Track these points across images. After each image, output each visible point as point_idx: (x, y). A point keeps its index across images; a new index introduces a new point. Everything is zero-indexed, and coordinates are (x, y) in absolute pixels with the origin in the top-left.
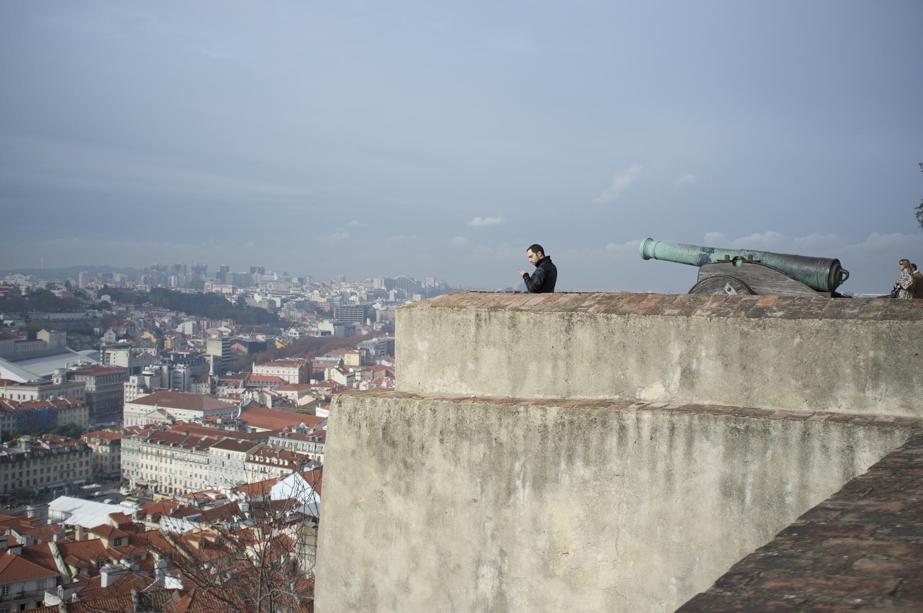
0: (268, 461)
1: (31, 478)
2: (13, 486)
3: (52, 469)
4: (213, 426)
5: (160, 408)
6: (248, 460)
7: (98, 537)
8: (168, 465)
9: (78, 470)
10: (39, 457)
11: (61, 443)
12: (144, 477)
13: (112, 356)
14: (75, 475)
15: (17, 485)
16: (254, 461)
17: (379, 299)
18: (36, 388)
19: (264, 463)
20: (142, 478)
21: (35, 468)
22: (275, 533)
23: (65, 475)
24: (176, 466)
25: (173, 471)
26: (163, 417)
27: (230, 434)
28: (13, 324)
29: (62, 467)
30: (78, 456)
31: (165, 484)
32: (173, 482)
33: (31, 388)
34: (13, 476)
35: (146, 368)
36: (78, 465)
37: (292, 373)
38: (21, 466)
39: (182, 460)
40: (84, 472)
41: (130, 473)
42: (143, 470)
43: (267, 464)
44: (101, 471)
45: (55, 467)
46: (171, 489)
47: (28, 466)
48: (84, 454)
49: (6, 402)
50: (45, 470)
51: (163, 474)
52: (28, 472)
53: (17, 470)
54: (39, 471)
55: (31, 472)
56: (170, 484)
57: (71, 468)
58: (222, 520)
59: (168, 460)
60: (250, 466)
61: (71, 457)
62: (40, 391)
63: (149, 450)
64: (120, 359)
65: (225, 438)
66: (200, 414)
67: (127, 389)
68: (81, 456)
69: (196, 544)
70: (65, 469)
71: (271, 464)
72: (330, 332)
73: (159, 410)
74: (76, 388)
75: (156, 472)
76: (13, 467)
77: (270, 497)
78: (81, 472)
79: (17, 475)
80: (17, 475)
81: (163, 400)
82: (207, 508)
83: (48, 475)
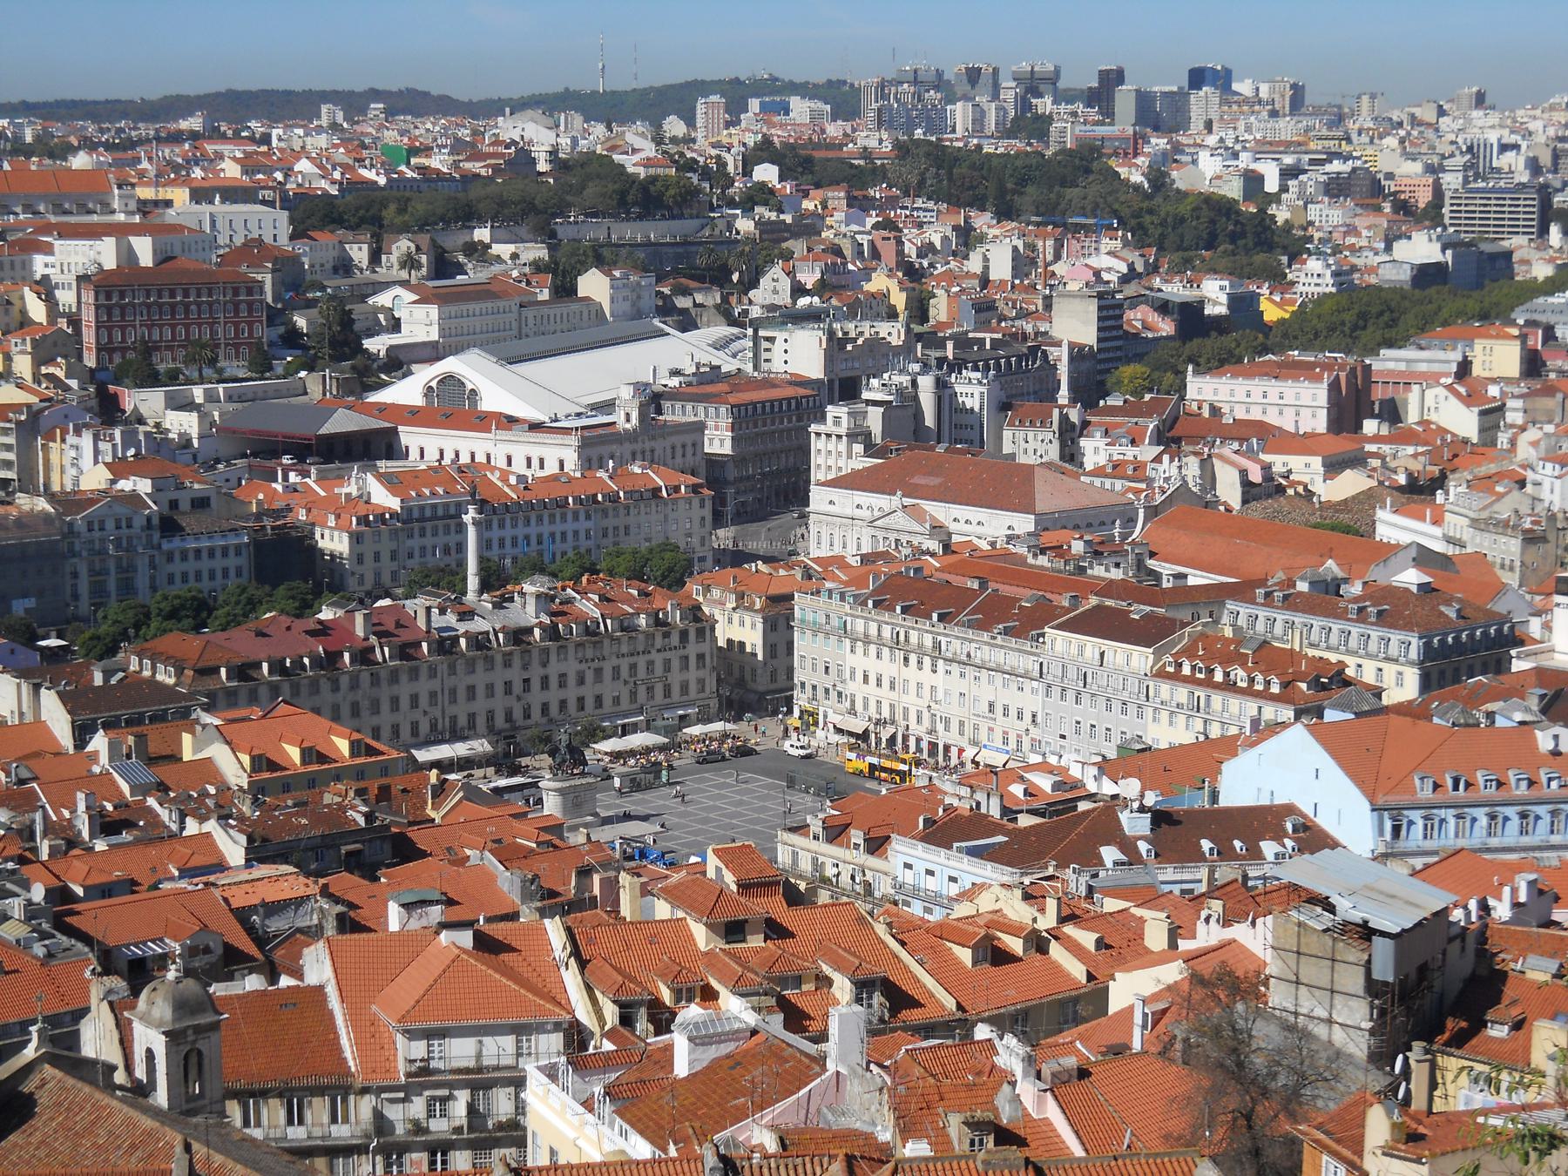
0: (1219, 677)
4: (1060, 564)
5: (907, 501)
6: (1161, 674)
7: (680, 914)
8: (926, 676)
9: (675, 678)
11: (629, 600)
12: (859, 707)
13: (779, 346)
14: (667, 692)
16: (1176, 677)
19: (1208, 683)
20: (852, 711)
21: (562, 668)
22: (1208, 935)
23: (642, 691)
24: (946, 681)
25: (940, 695)
26: (918, 528)
27: (1109, 588)
28: (515, 256)
31: (917, 730)
32: (940, 727)
33: (559, 439)
35: (874, 382)
36: (676, 664)
39: (968, 662)
40: (693, 687)
41: (820, 693)
42: (854, 687)
43: (1217, 686)
44: (741, 683)
45: (616, 671)
46: (933, 747)
49: (494, 478)
50: (589, 676)
51: (912, 701)
54: (572, 680)
56: (931, 732)
58: (1062, 866)
59: (927, 661)
60: (1165, 688)
63: (873, 630)
64: (800, 355)
65: (1094, 600)
66: (1024, 523)
67: (816, 444)
69: (965, 955)
70: (642, 673)
71: (1229, 686)
74: (677, 440)
75: (893, 695)
77: (1214, 796)
78: (685, 688)
79: (517, 687)
80: (517, 687)
81: (918, 480)
82: (1025, 821)
83: (598, 689)
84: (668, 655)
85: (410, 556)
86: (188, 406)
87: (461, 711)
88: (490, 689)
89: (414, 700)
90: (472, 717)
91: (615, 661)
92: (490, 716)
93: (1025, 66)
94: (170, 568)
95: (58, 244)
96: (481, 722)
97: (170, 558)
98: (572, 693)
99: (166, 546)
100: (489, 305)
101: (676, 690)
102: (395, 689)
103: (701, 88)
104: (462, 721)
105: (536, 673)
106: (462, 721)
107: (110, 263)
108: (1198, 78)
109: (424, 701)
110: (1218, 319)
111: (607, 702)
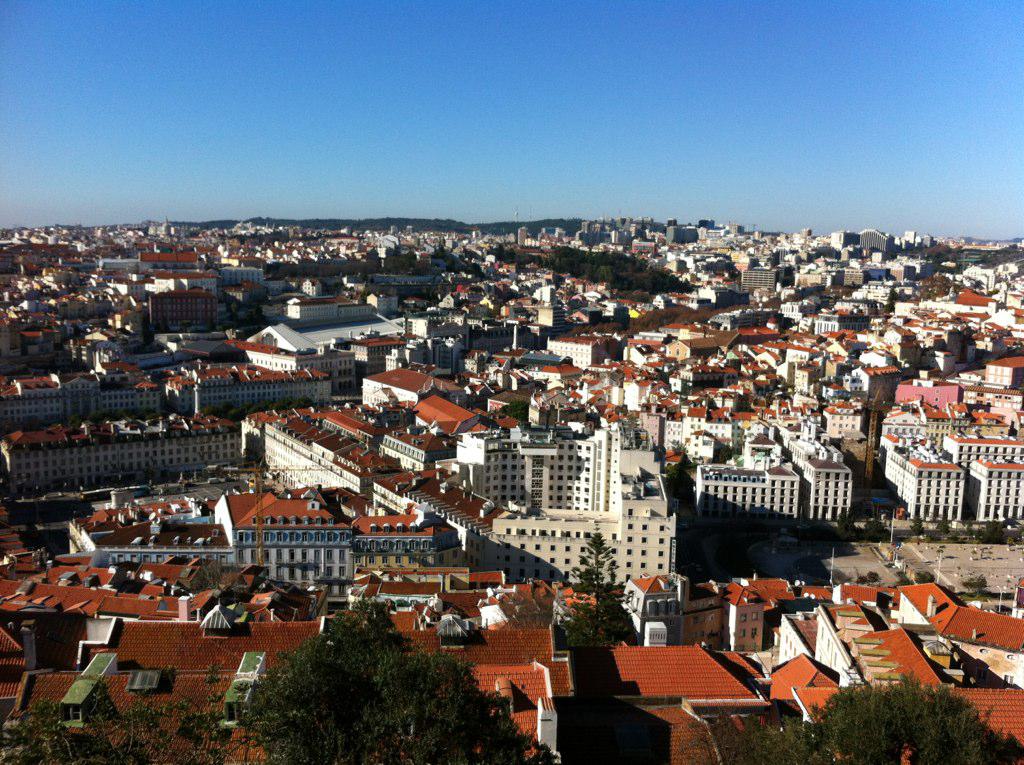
1: (167, 457)
2: (147, 464)
9: (221, 452)
10: (175, 437)
17: (822, 258)
18: (294, 359)
21: (171, 447)
23: (206, 456)
29: (202, 448)
30: (221, 437)
36: (221, 447)
37: (585, 351)
38: (155, 446)
39: (298, 452)
45: (195, 449)
47: (163, 445)
48: (228, 436)
50: (183, 451)
53: (150, 449)
54: (175, 451)
55: (167, 453)
57: (213, 449)
61: (213, 438)
62: (297, 361)
68: (225, 438)
70: (206, 450)
72: (709, 300)
73: (383, 389)
74: (343, 359)
76: (147, 446)
79: (151, 454)
80: (151, 454)
86: (177, 341)
93: (640, 219)
94: (104, 402)
95: (156, 281)
99: (102, 394)
100: (323, 306)
102: (98, 454)
103: (520, 225)
105: (159, 449)
107: (173, 288)
108: (703, 224)
110: (608, 318)
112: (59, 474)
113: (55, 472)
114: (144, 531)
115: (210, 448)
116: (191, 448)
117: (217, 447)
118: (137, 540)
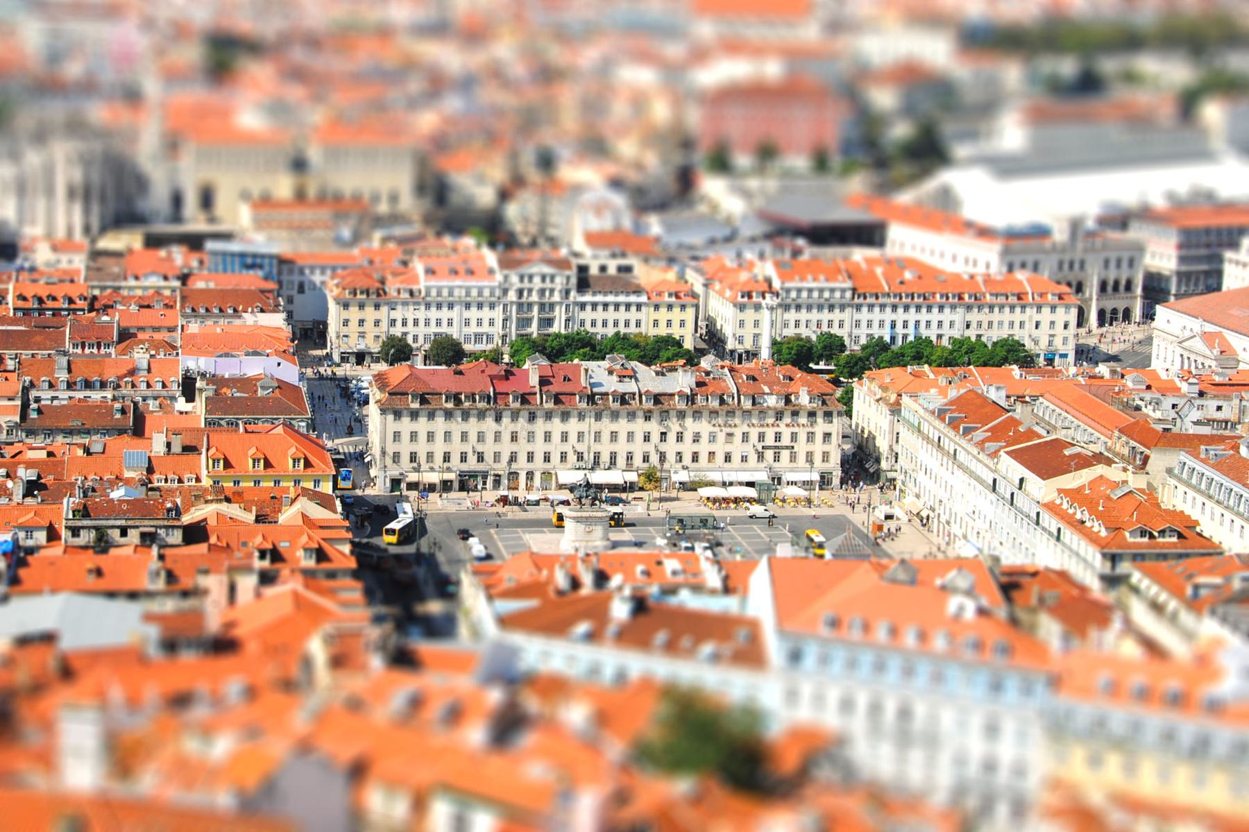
2: (646, 459)
3: (738, 438)
9: (802, 447)
14: (793, 458)
15: (654, 459)
23: (769, 454)
29: (761, 437)
34: (647, 438)
36: (802, 437)
52: (680, 437)
53: (654, 427)
57: (786, 441)
62: (1006, 252)
79: (655, 437)
83: (728, 448)
84: (796, 430)
85: (786, 325)
87: (605, 449)
88: (630, 436)
89: (565, 437)
90: (613, 457)
91: (745, 429)
92: (630, 457)
96: (621, 461)
97: (583, 306)
98: (704, 448)
101: (802, 458)
104: (605, 458)
106: (605, 458)
109: (573, 438)
111: (736, 458)
112: (472, 464)
113: (464, 458)
114: (597, 612)
115: (778, 437)
116: (738, 433)
117: (794, 437)
118: (582, 628)
